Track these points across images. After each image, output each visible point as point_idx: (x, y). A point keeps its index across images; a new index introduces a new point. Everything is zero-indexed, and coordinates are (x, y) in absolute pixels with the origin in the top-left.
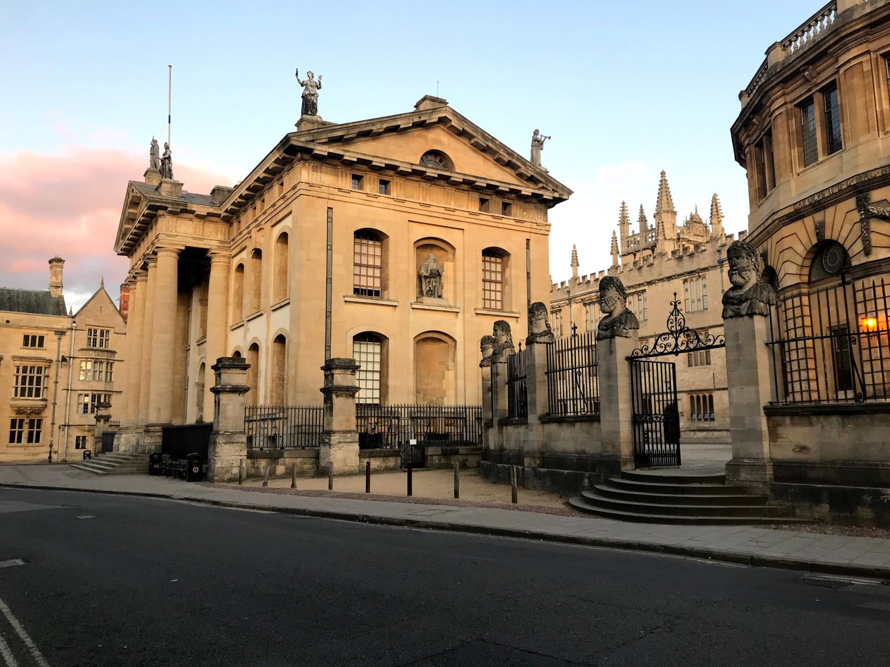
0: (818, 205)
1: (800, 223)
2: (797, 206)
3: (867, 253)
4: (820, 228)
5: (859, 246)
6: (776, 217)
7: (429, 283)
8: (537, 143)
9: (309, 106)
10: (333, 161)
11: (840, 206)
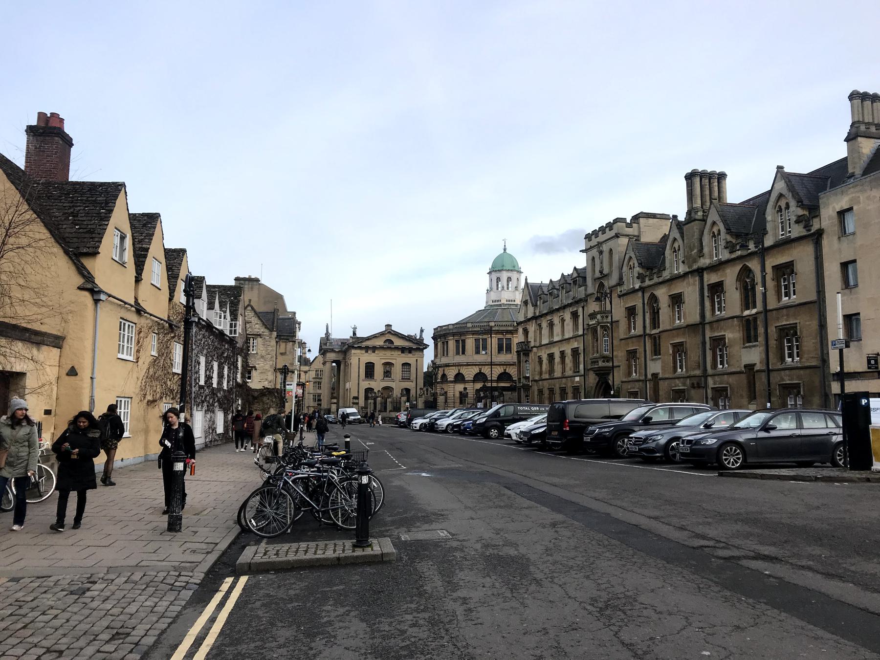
7: (387, 374)
8: (422, 331)
9: (354, 334)
10: (360, 348)
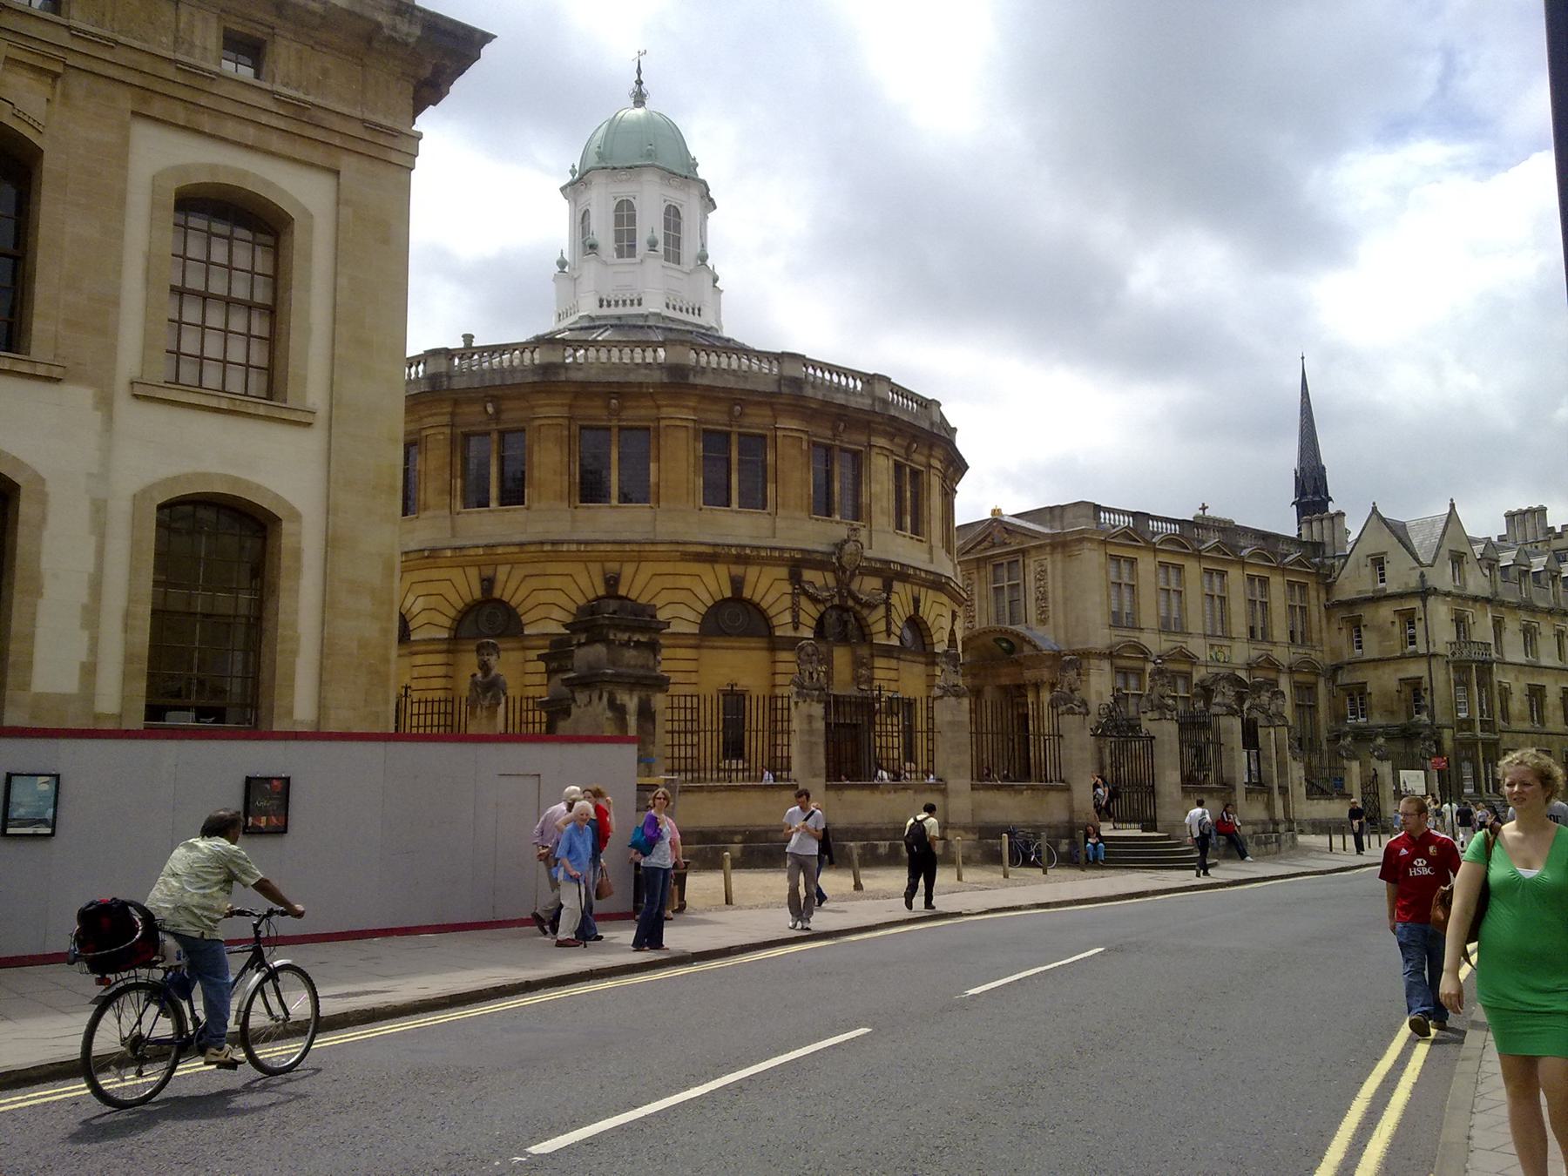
0: (743, 557)
1: (707, 566)
2: (719, 550)
3: (796, 628)
4: (737, 583)
5: (787, 617)
6: (681, 548)
11: (767, 569)
